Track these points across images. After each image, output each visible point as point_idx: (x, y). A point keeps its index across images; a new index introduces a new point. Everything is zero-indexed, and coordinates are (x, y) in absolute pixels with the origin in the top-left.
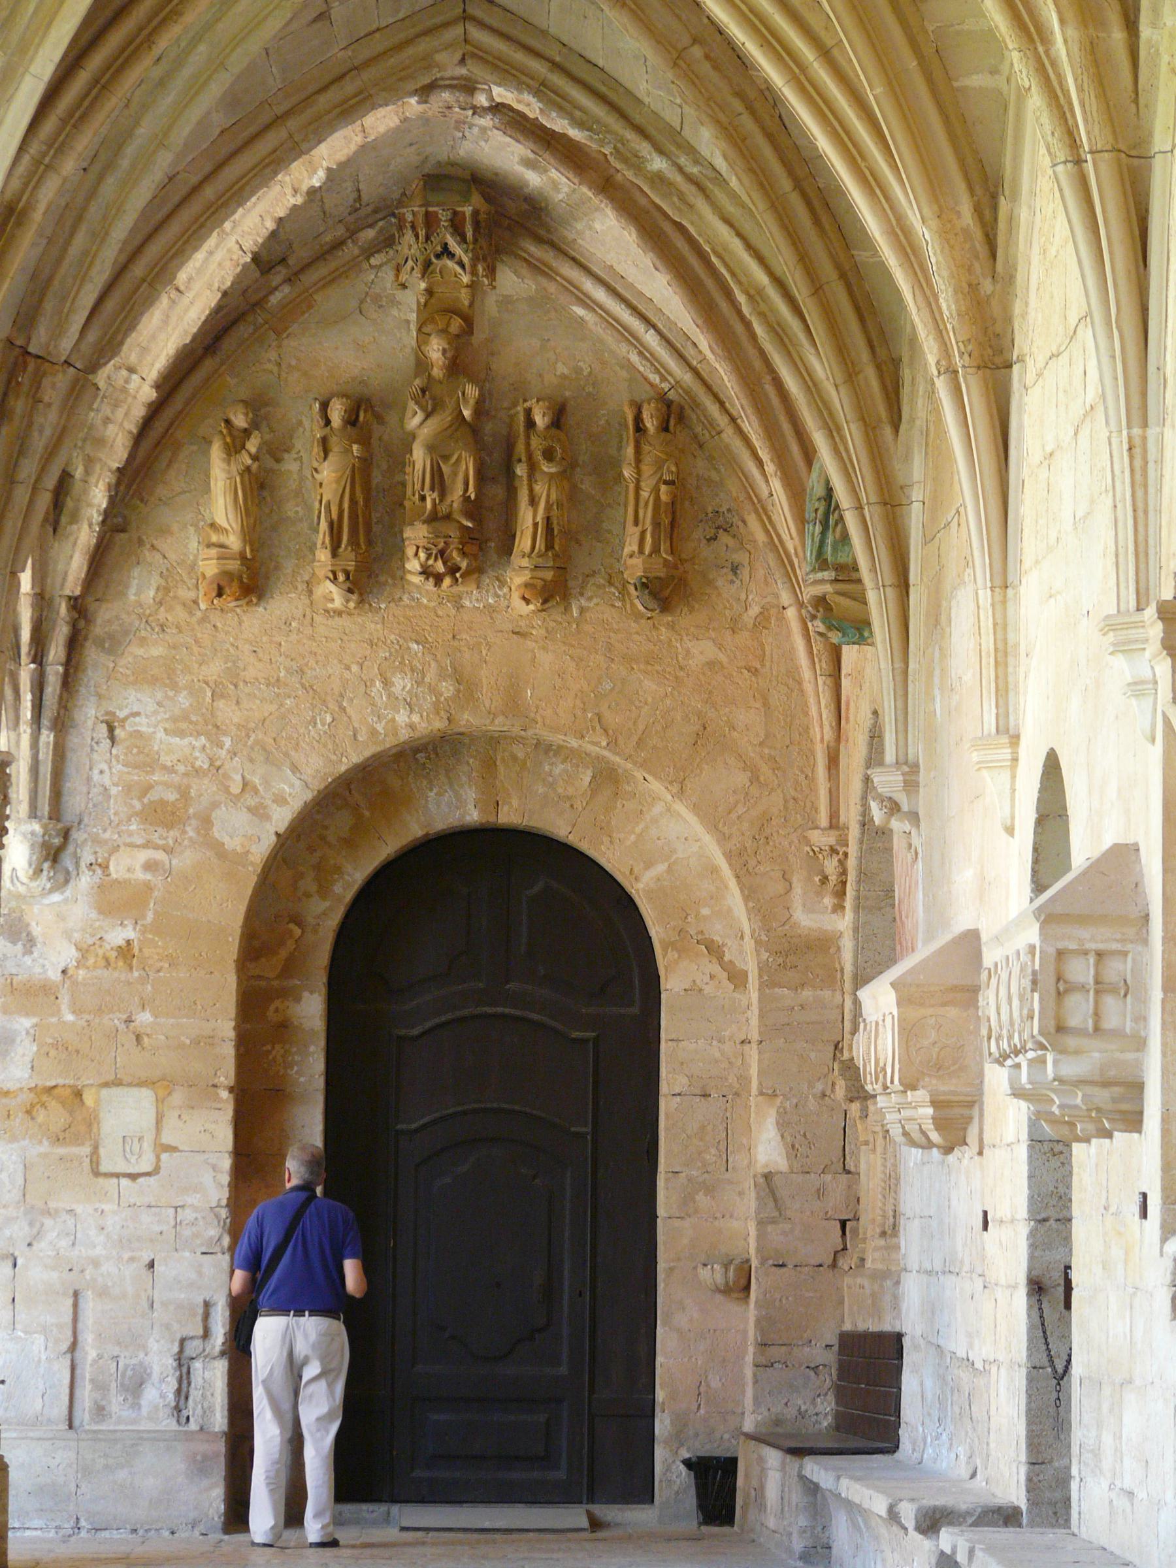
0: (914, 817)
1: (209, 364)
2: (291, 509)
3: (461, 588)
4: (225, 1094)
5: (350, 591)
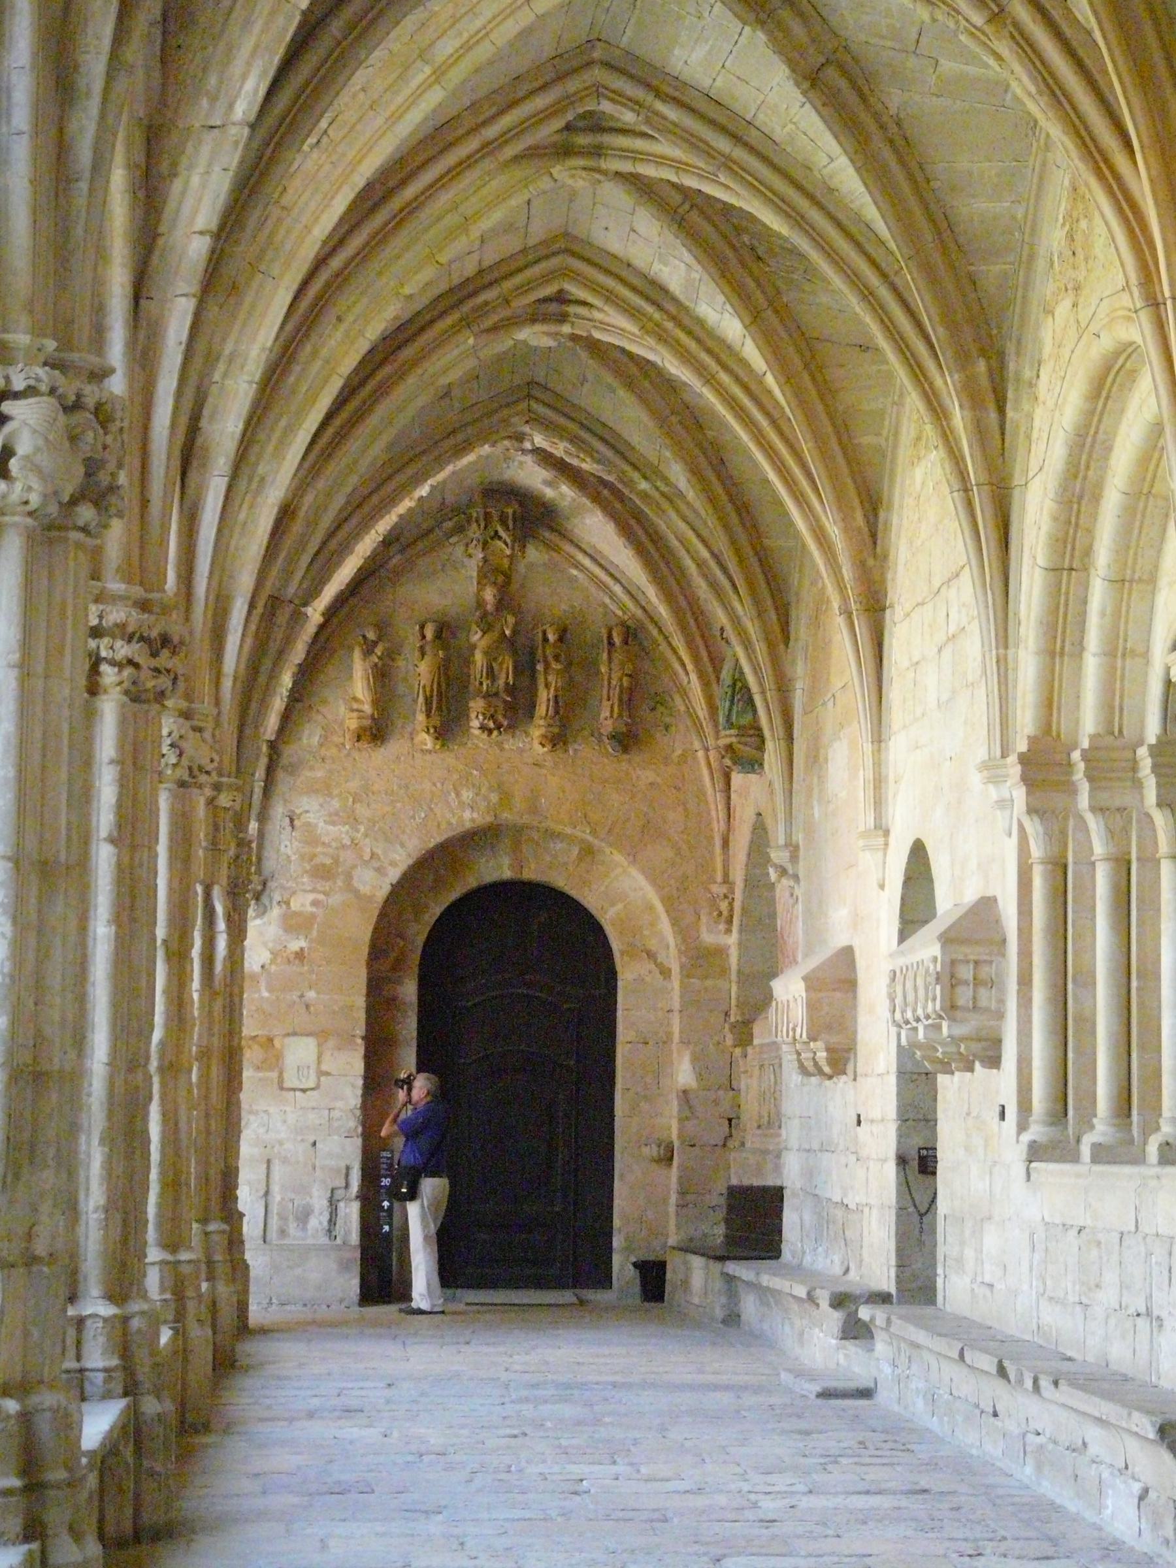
0: (796, 877)
1: (353, 601)
2: (401, 689)
3: (503, 737)
4: (359, 1041)
5: (437, 738)
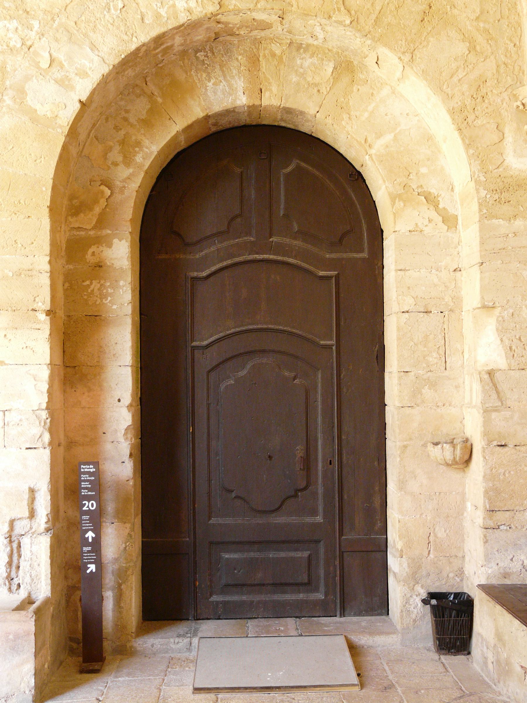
4: (42, 317)
